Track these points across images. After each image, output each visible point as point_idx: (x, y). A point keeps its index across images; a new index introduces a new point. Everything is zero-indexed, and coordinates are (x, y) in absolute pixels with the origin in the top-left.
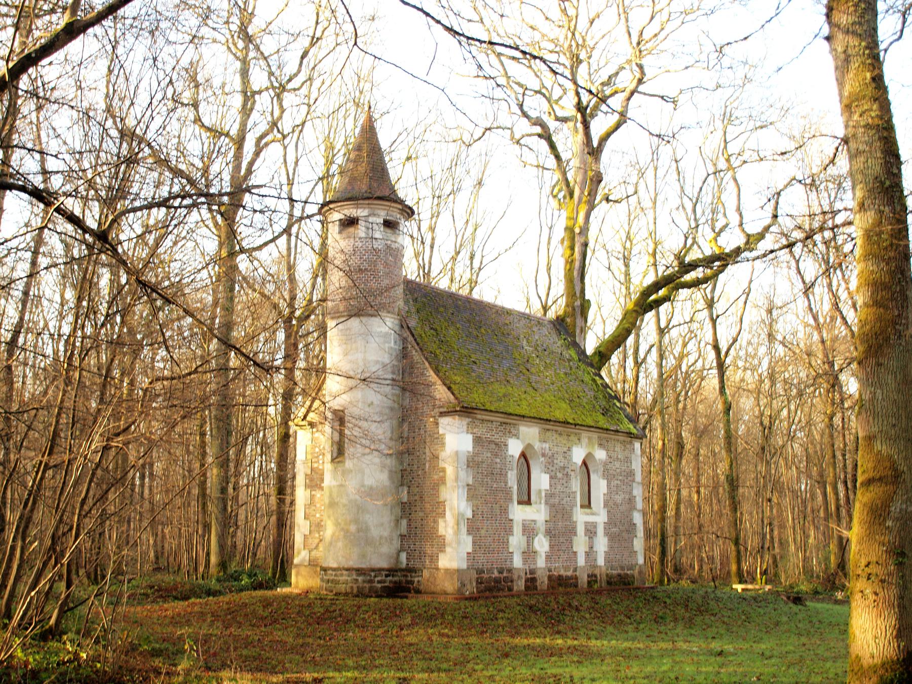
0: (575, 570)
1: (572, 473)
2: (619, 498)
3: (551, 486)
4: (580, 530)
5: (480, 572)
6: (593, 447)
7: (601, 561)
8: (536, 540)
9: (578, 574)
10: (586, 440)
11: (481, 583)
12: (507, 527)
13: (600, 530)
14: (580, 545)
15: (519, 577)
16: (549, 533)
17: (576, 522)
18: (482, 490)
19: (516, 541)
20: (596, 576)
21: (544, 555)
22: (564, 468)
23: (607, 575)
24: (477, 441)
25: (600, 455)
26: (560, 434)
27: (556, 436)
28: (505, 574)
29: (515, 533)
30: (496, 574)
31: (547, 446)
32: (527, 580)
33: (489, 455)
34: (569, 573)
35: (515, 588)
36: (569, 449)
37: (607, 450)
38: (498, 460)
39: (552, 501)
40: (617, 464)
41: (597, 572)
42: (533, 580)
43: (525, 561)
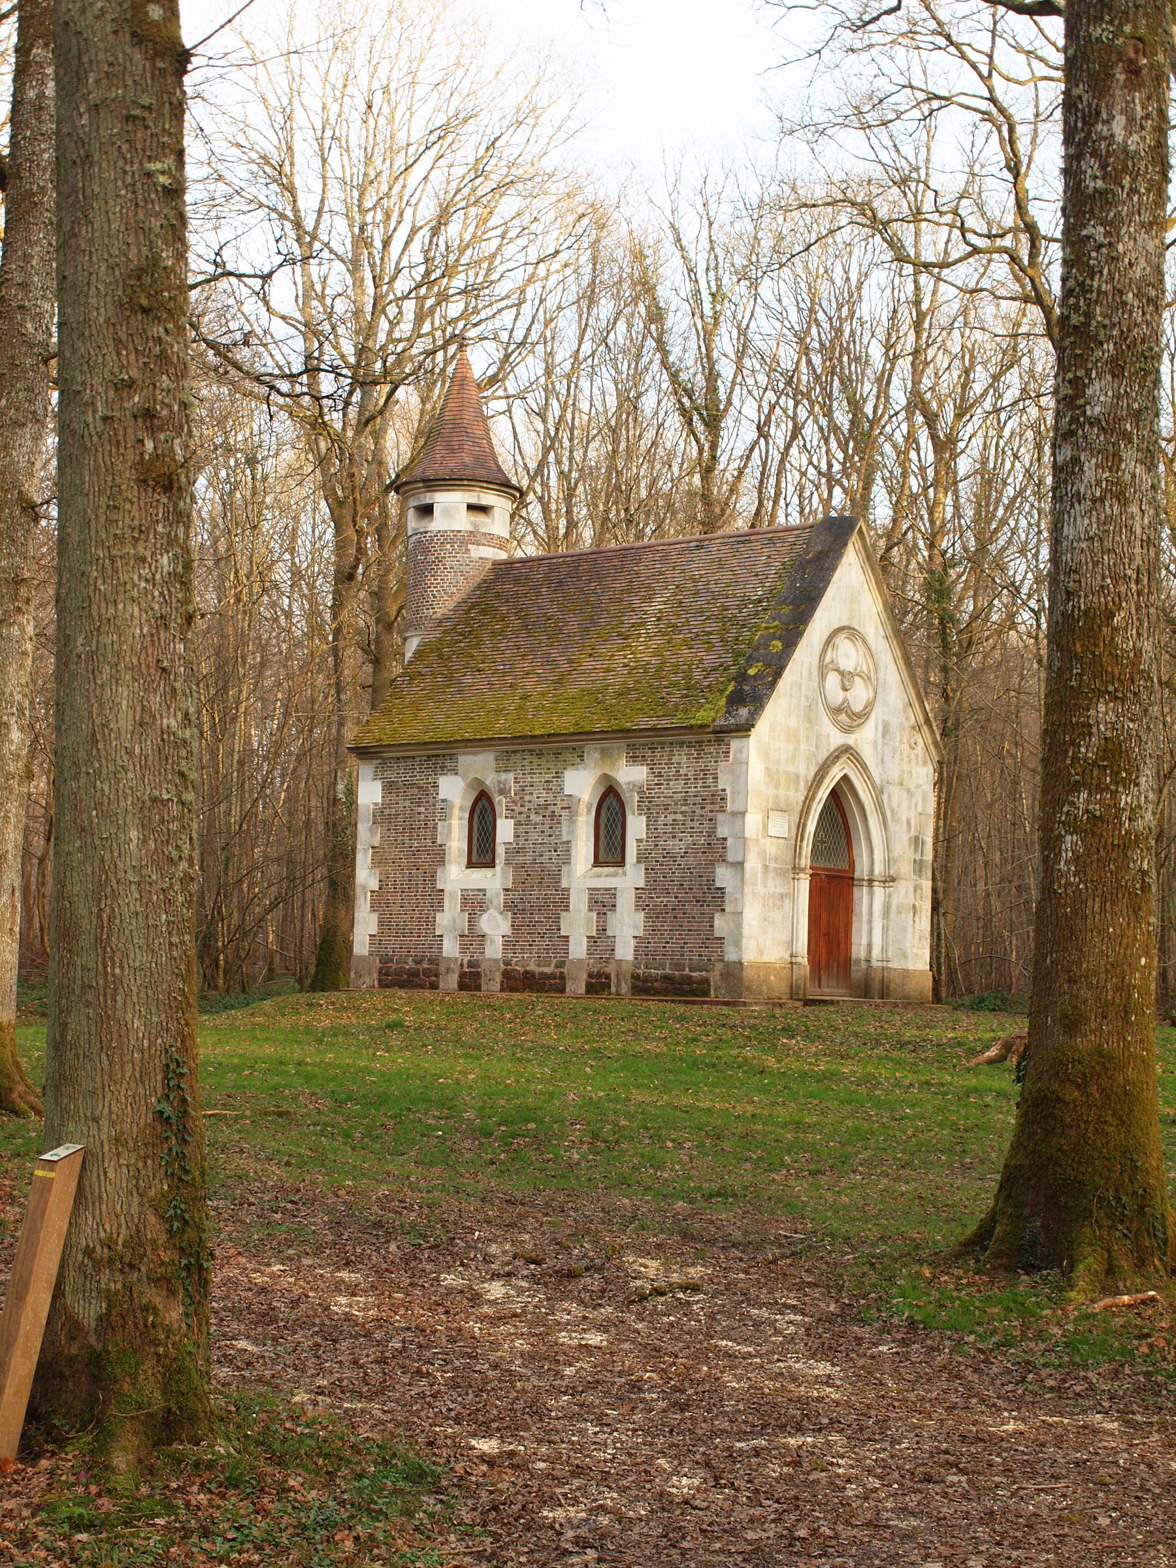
0: (561, 964)
2: (677, 846)
3: (517, 836)
4: (579, 902)
5: (385, 960)
6: (613, 765)
7: (625, 951)
8: (485, 917)
10: (597, 755)
11: (387, 974)
12: (437, 899)
13: (626, 902)
14: (577, 927)
15: (448, 969)
16: (510, 907)
17: (568, 890)
18: (395, 853)
19: (449, 919)
20: (608, 977)
21: (499, 941)
22: (546, 806)
23: (636, 977)
24: (389, 787)
25: (631, 775)
26: (540, 754)
27: (535, 760)
29: (446, 908)
30: (410, 964)
31: (511, 776)
32: (463, 975)
33: (408, 804)
35: (441, 985)
36: (558, 775)
38: (422, 809)
39: (520, 859)
40: (679, 786)
41: (611, 969)
42: (477, 976)
43: (464, 949)
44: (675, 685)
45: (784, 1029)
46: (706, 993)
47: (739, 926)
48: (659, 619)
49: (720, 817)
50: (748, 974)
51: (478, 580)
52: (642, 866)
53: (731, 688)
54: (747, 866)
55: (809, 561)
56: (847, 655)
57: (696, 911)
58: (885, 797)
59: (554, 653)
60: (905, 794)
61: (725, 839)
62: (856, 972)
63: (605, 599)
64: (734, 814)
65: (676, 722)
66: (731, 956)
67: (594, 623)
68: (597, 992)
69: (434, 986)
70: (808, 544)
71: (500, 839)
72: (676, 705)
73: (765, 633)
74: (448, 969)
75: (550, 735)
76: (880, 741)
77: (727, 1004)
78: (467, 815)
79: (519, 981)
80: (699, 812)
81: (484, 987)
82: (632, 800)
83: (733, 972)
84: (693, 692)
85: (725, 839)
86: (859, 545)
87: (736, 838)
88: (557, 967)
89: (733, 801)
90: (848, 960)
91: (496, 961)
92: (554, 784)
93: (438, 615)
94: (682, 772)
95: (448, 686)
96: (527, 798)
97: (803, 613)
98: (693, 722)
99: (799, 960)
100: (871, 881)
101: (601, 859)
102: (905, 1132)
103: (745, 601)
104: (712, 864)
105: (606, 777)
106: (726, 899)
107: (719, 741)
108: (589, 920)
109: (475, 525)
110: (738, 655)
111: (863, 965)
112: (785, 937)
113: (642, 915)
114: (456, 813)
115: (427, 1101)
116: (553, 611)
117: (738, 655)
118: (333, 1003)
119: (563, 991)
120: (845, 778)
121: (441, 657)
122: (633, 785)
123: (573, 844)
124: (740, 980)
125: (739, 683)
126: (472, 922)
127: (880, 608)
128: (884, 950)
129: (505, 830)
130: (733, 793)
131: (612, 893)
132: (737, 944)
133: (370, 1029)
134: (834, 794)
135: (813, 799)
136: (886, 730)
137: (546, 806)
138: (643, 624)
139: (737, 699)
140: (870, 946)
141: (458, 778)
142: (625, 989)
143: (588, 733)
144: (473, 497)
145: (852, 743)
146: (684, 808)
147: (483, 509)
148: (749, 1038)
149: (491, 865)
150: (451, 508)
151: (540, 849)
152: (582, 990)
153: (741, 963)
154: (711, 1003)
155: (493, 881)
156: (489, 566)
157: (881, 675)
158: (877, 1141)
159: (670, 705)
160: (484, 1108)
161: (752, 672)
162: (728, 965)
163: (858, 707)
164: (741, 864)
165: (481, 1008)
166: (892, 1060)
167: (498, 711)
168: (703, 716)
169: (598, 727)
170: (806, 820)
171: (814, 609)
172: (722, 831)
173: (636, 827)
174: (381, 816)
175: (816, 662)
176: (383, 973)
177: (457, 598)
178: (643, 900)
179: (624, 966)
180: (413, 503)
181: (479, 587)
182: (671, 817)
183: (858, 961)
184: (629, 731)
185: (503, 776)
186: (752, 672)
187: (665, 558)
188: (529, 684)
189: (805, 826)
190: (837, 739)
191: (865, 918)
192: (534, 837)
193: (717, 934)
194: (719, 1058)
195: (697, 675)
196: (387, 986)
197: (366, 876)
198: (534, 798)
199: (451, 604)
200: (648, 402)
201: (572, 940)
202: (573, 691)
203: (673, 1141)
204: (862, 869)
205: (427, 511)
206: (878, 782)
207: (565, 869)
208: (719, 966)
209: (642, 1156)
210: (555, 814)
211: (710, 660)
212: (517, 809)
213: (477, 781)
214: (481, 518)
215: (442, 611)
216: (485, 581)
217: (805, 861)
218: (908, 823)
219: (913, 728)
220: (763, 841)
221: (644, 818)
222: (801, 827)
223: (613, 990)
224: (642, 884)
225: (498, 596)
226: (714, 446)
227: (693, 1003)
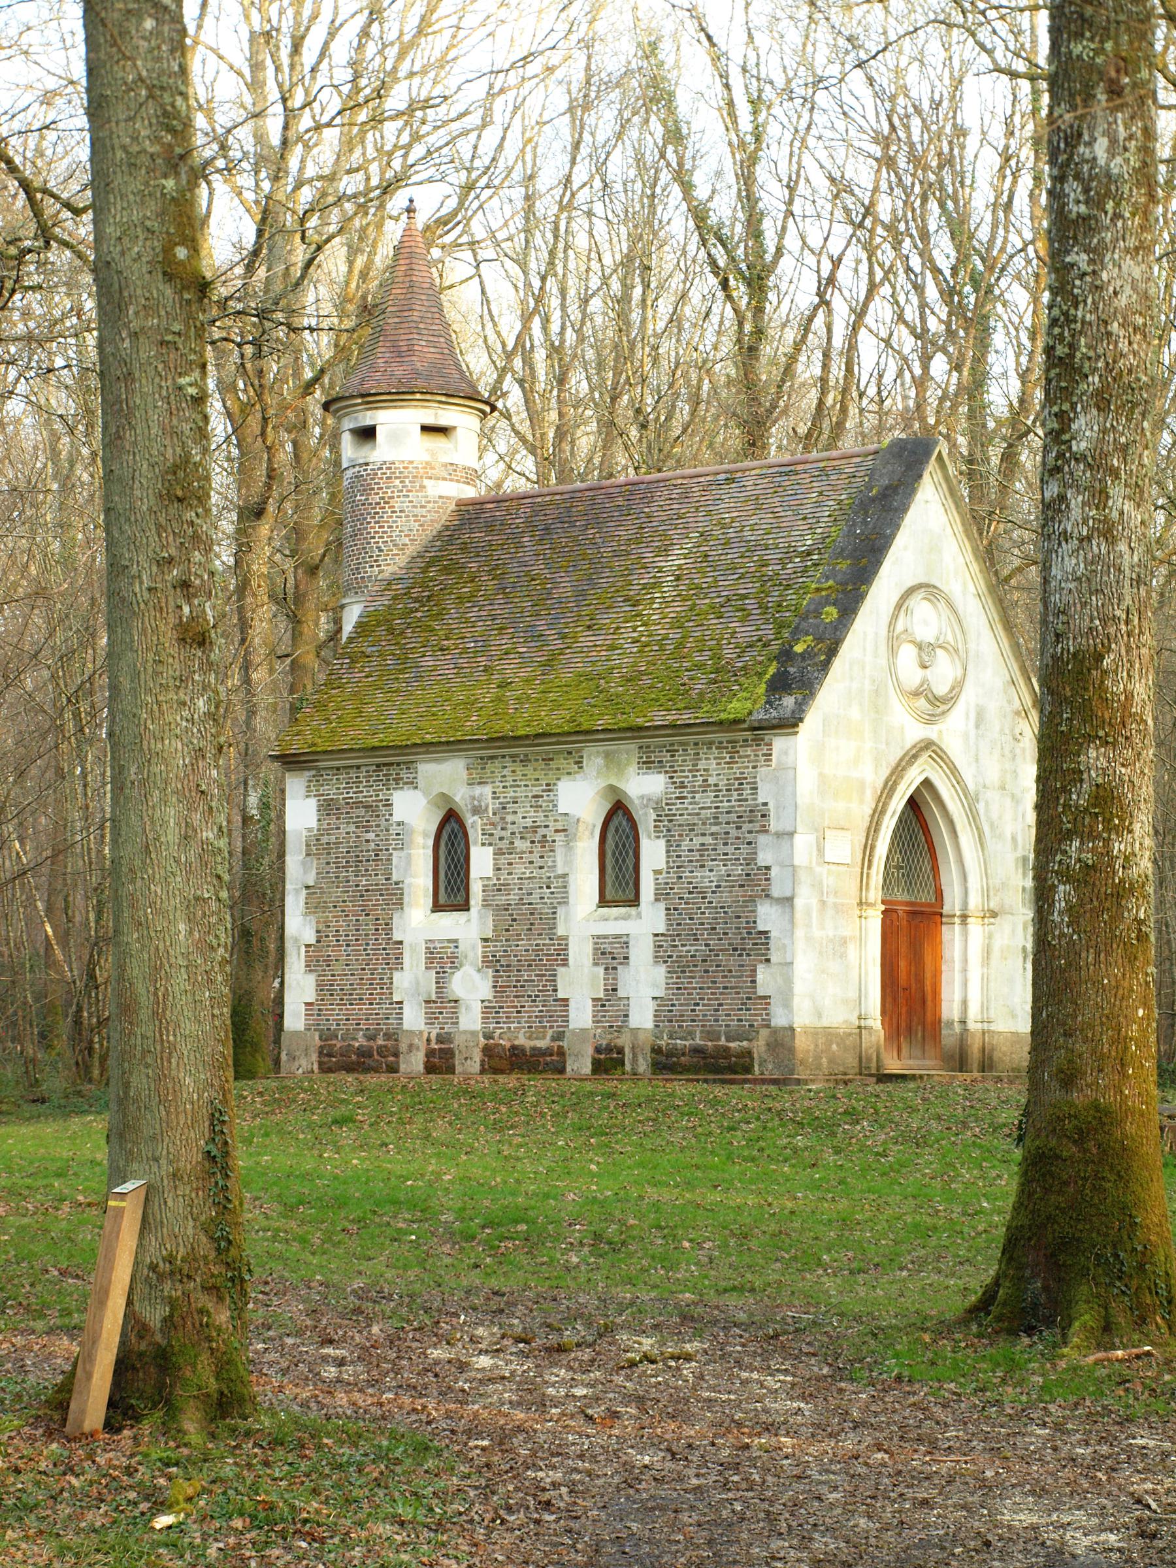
0: (559, 1036)
1: (559, 837)
2: (706, 878)
4: (580, 953)
5: (327, 1036)
6: (621, 770)
7: (642, 1017)
9: (565, 1044)
10: (600, 761)
11: (330, 1055)
12: (394, 954)
13: (642, 952)
14: (579, 985)
15: (411, 1046)
16: (491, 962)
17: (566, 938)
18: (337, 893)
19: (410, 982)
20: (620, 1051)
21: (477, 1008)
22: (534, 830)
23: (657, 1050)
24: (327, 808)
25: (644, 787)
26: (525, 761)
28: (380, 1042)
30: (360, 1041)
31: (487, 790)
32: (430, 1053)
33: (352, 828)
34: (542, 1044)
35: (403, 1067)
36: (549, 787)
37: (671, 773)
38: (371, 836)
40: (706, 800)
41: (624, 1041)
43: (431, 1018)
44: (699, 666)
45: (846, 1112)
46: (748, 1069)
47: (789, 981)
48: (678, 578)
49: (762, 839)
50: (802, 1043)
51: (438, 527)
52: (662, 906)
53: (772, 670)
54: (799, 902)
55: (873, 500)
56: (925, 620)
57: (733, 962)
58: (981, 807)
59: (541, 625)
60: (1008, 802)
61: (768, 868)
62: (949, 1038)
63: (606, 551)
64: (779, 835)
65: (701, 716)
66: (779, 1019)
67: (593, 585)
68: (607, 1071)
69: (393, 1069)
70: (871, 476)
71: (474, 874)
72: (702, 694)
73: (816, 596)
74: (411, 1046)
75: (538, 736)
76: (972, 732)
77: (774, 1082)
78: (431, 842)
79: (504, 1060)
80: (734, 833)
81: (458, 1069)
82: (646, 820)
83: (782, 1041)
84: (724, 676)
85: (768, 868)
86: (938, 476)
87: (782, 865)
88: (553, 1039)
89: (778, 819)
90: (936, 1024)
91: (474, 1033)
92: (544, 799)
93: (386, 575)
94: (712, 781)
95: (402, 671)
96: (509, 818)
97: (865, 568)
98: (723, 716)
99: (870, 1022)
100: (964, 917)
101: (608, 897)
102: (974, 1228)
103: (790, 553)
104: (752, 900)
105: (612, 789)
106: (772, 946)
107: (758, 741)
108: (594, 977)
109: (433, 454)
110: (781, 626)
111: (957, 1028)
112: (853, 994)
113: (662, 970)
114: (419, 840)
115: (396, 1202)
116: (539, 568)
117: (781, 626)
118: (261, 1094)
119: (562, 1071)
120: (927, 783)
121: (391, 630)
122: (647, 800)
123: (571, 878)
124: (792, 1050)
125: (783, 664)
126: (441, 984)
127: (970, 557)
128: (985, 1007)
129: (482, 862)
130: (777, 808)
131: (624, 942)
132: (787, 1004)
133: (311, 1126)
134: (913, 803)
135: (883, 812)
136: (980, 719)
137: (534, 830)
138: (657, 585)
139: (779, 685)
140: (965, 1003)
141: (418, 794)
142: (643, 1066)
143: (587, 732)
144: (430, 415)
145: (934, 737)
146: (714, 829)
147: (442, 430)
148: (800, 1124)
149: (465, 907)
150: (398, 426)
151: (527, 885)
152: (587, 1069)
153: (792, 1029)
154: (755, 1081)
155: (468, 928)
156: (453, 507)
157: (972, 646)
158: (940, 1239)
159: (694, 693)
160: (464, 1209)
161: (799, 648)
162: (775, 1031)
163: (941, 690)
164: (789, 901)
165: (456, 1096)
166: (981, 1147)
167: (469, 704)
168: (736, 707)
169: (600, 724)
170: (875, 839)
171: (878, 563)
172: (764, 857)
173: (653, 854)
174: (317, 846)
175: (884, 632)
176: (325, 1053)
177: (411, 551)
178: (663, 949)
179: (642, 1037)
180: (348, 424)
181: (439, 536)
182: (697, 841)
183: (950, 1024)
184: (640, 729)
185: (478, 790)
186: (799, 648)
187: (686, 495)
188: (509, 667)
189: (873, 848)
190: (916, 732)
191: (958, 966)
192: (519, 869)
193: (761, 992)
194: (761, 1150)
195: (728, 653)
196: (330, 1070)
197: (299, 926)
198: (518, 818)
199: (402, 560)
200: (665, 261)
201: (572, 1004)
202: (567, 676)
203: (691, 1241)
204: (952, 903)
205: (367, 434)
206: (971, 787)
207: (561, 911)
208: (764, 1033)
209: (653, 1258)
210: (544, 838)
211: (745, 633)
212: (498, 833)
213: (444, 796)
214: (438, 441)
215: (391, 569)
216: (447, 528)
217: (875, 893)
218: (1014, 839)
219: (1018, 713)
220: (818, 869)
221: (662, 843)
222: (868, 849)
223: (628, 1067)
224: (662, 929)
225: (464, 548)
226: (759, 311)
227: (732, 1082)
